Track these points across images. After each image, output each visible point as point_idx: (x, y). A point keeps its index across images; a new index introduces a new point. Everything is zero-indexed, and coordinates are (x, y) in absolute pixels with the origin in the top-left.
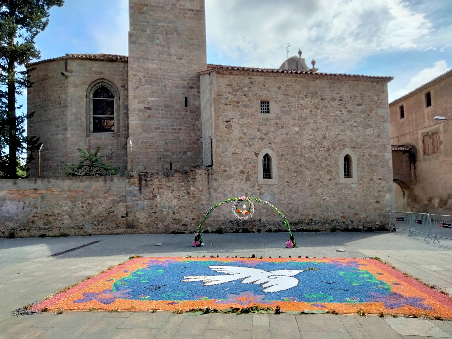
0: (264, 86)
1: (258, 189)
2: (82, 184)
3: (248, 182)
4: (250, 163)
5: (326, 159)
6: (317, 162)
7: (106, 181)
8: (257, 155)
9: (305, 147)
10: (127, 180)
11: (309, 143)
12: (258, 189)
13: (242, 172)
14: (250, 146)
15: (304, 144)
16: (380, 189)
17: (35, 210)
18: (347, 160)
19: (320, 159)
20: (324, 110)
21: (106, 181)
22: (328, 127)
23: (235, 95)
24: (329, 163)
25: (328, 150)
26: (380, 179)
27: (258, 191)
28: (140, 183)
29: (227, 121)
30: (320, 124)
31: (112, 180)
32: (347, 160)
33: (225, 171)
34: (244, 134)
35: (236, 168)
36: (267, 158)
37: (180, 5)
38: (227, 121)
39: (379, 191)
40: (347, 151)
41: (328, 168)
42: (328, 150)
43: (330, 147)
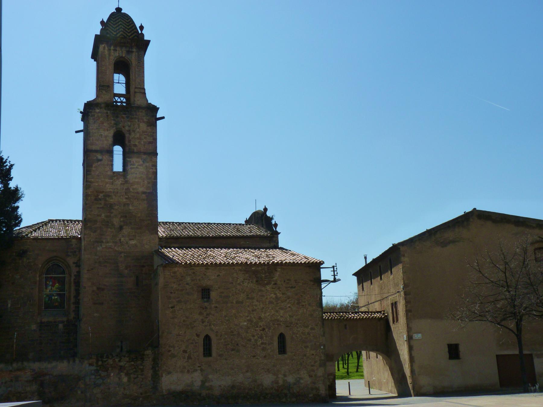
0: (205, 275)
1: (199, 367)
2: (49, 366)
3: (190, 361)
4: (192, 343)
5: (261, 338)
6: (253, 340)
7: (69, 362)
8: (198, 336)
9: (241, 328)
10: (86, 362)
11: (245, 324)
12: (199, 367)
13: (185, 351)
14: (192, 328)
15: (242, 324)
16: (313, 364)
17: (9, 389)
18: (282, 337)
19: (256, 337)
20: (260, 294)
21: (69, 362)
22: (263, 308)
23: (179, 285)
24: (265, 341)
25: (264, 329)
26: (313, 355)
27: (199, 368)
28: (97, 363)
29: (172, 307)
30: (256, 306)
31: (74, 361)
32: (282, 337)
33: (169, 351)
34: (187, 317)
35: (179, 348)
36: (207, 338)
37: (133, 189)
38: (172, 307)
39: (312, 366)
40: (282, 330)
41: (263, 346)
42: (264, 329)
43: (265, 327)
